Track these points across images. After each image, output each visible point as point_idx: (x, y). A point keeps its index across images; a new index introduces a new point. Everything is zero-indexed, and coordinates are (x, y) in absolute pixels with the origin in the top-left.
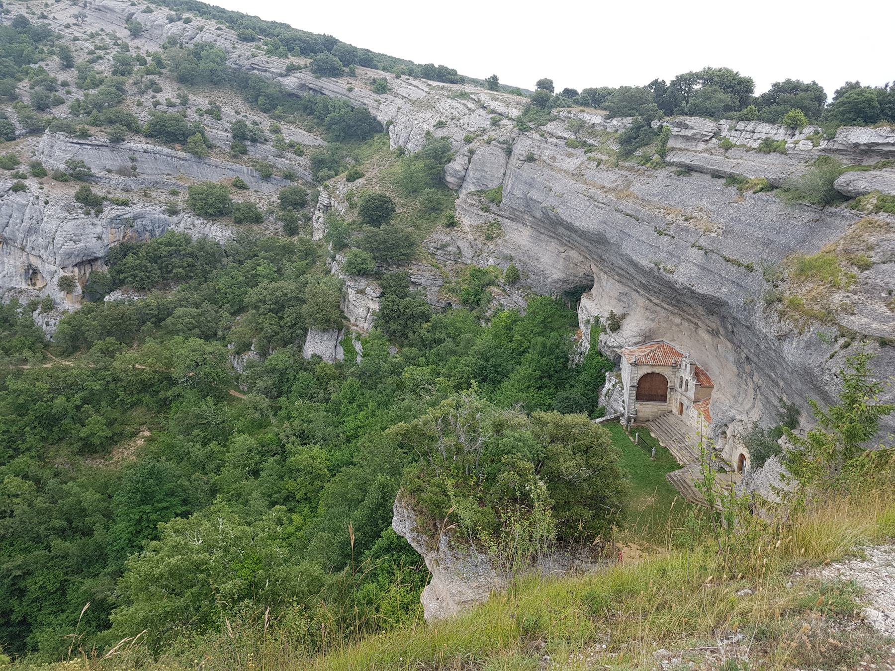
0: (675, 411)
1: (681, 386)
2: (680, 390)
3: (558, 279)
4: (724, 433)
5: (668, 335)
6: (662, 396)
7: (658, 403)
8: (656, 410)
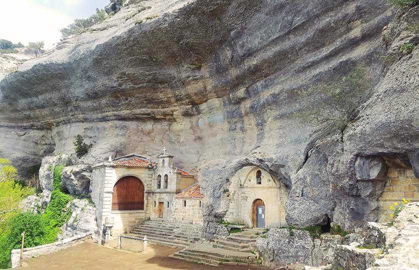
0: (154, 216)
1: (159, 185)
2: (158, 190)
4: (226, 191)
6: (138, 203)
7: (135, 211)
8: (133, 219)
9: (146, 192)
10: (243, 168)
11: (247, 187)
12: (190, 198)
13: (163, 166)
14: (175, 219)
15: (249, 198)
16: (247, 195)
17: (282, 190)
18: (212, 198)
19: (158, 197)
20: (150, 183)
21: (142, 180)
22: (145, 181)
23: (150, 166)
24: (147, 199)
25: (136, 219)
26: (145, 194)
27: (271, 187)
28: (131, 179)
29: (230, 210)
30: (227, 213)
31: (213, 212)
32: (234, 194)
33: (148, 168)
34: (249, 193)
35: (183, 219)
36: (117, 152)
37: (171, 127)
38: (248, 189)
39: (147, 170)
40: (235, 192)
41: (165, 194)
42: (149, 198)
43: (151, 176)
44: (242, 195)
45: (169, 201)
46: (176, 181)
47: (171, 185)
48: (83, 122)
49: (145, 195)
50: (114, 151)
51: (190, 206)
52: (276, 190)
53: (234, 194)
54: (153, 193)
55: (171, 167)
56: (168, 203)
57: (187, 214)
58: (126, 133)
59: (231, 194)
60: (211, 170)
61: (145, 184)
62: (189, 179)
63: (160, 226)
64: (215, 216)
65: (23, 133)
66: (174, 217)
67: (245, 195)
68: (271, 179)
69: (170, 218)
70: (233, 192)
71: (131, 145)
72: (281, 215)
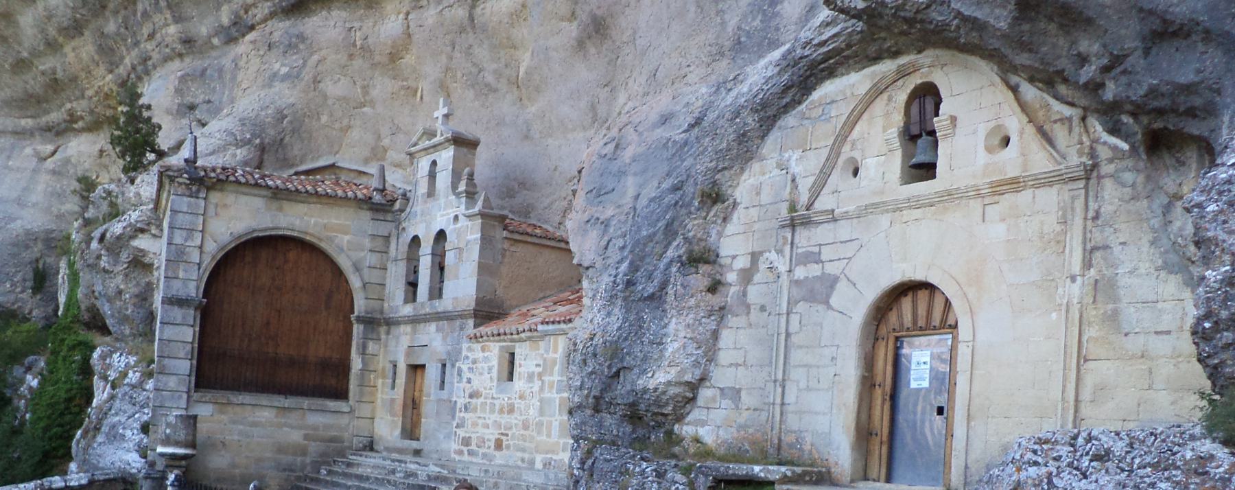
0: (387, 429)
1: (413, 285)
2: (408, 310)
3: (28, 233)
5: (355, 134)
7: (306, 402)
8: (296, 437)
9: (359, 319)
10: (816, 95)
11: (833, 217)
12: (534, 336)
13: (431, 193)
14: (466, 442)
15: (842, 286)
16: (831, 269)
17: (1110, 190)
18: (617, 312)
19: (405, 342)
20: (373, 277)
21: (344, 263)
22: (357, 268)
23: (377, 197)
24: (363, 351)
25: (306, 437)
26: (355, 327)
27: (1015, 184)
28: (292, 255)
29: (722, 376)
30: (705, 394)
31: (621, 390)
32: (747, 276)
33: (366, 203)
34: (848, 251)
35: (499, 445)
36: (262, 149)
37: (478, 10)
38: (844, 230)
39: (366, 215)
40: (755, 257)
41: (432, 327)
42: (371, 347)
43: (379, 243)
44: (800, 273)
45: (444, 357)
46: (475, 254)
47: (457, 277)
48: (180, 55)
49: (357, 329)
50: (249, 142)
51: (530, 377)
52: (1050, 198)
53: (747, 276)
54: (390, 323)
55: (462, 187)
56: (444, 366)
57: (514, 419)
58: (304, 65)
59: (731, 277)
60: (628, 154)
61: (355, 282)
62: (547, 252)
63: (393, 472)
64: (634, 416)
65: (50, 148)
66: (462, 433)
67: (814, 270)
68: (1014, 123)
69: (448, 436)
70: (742, 263)
71: (324, 119)
72: (1089, 381)
